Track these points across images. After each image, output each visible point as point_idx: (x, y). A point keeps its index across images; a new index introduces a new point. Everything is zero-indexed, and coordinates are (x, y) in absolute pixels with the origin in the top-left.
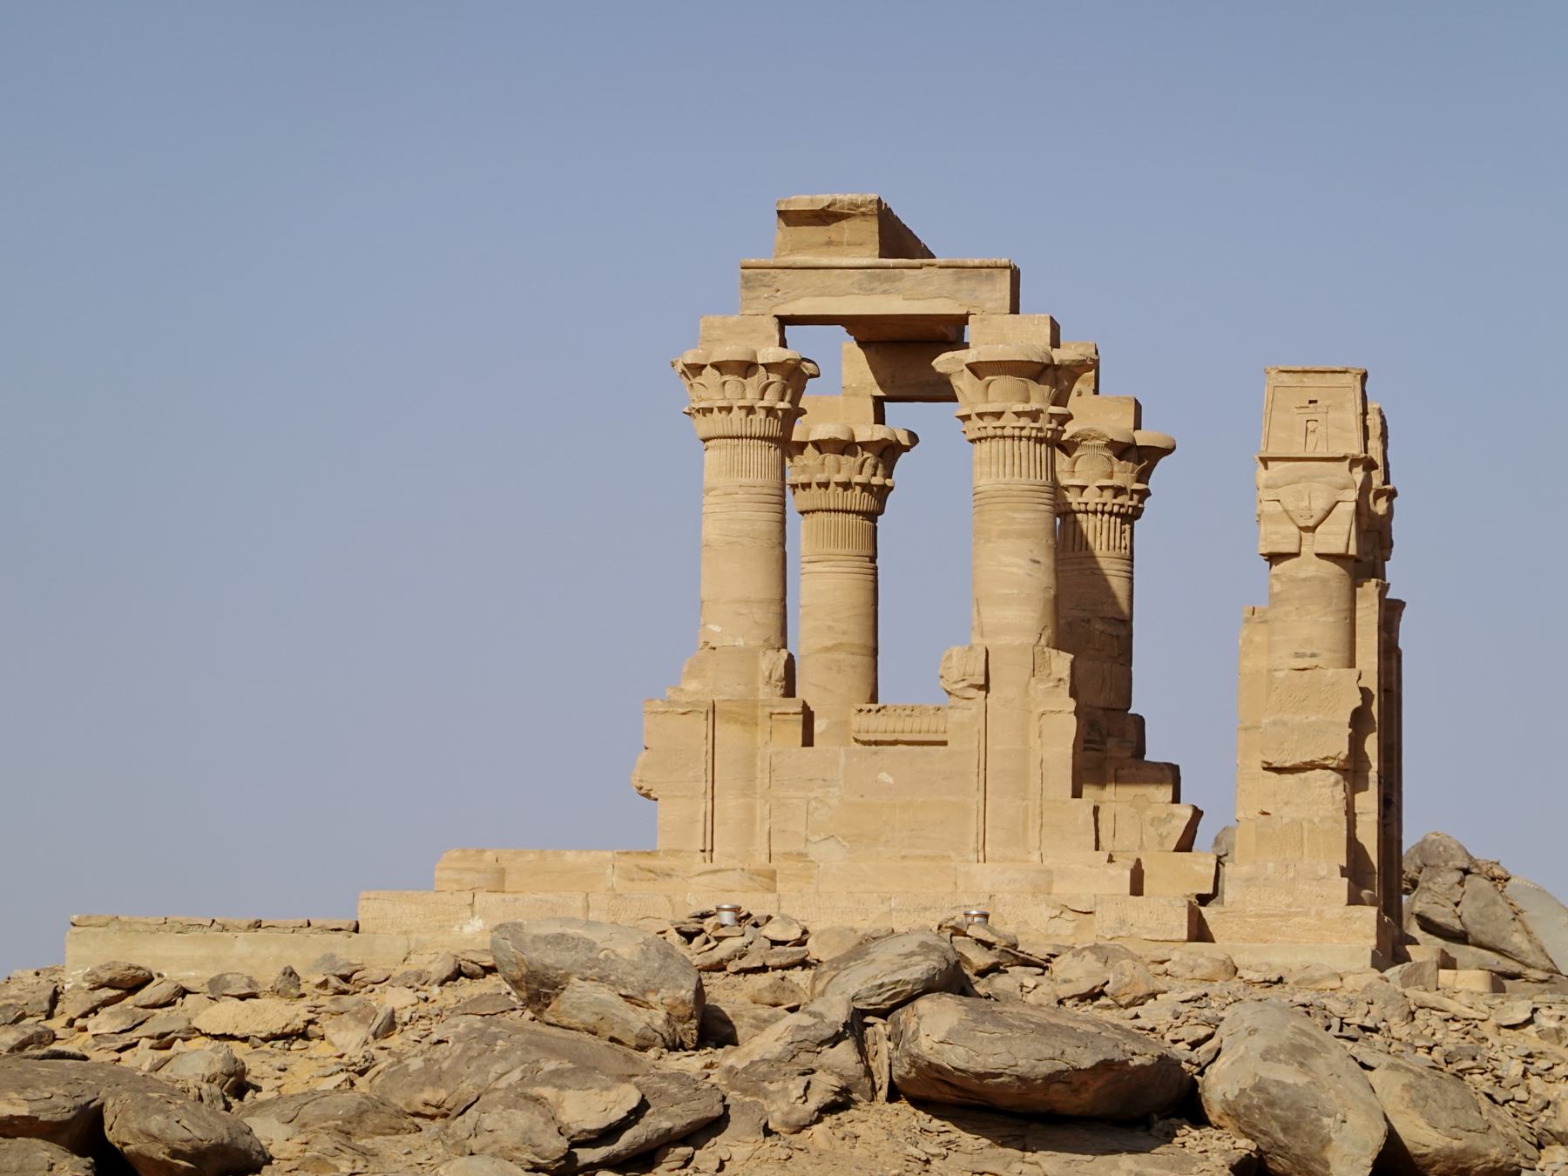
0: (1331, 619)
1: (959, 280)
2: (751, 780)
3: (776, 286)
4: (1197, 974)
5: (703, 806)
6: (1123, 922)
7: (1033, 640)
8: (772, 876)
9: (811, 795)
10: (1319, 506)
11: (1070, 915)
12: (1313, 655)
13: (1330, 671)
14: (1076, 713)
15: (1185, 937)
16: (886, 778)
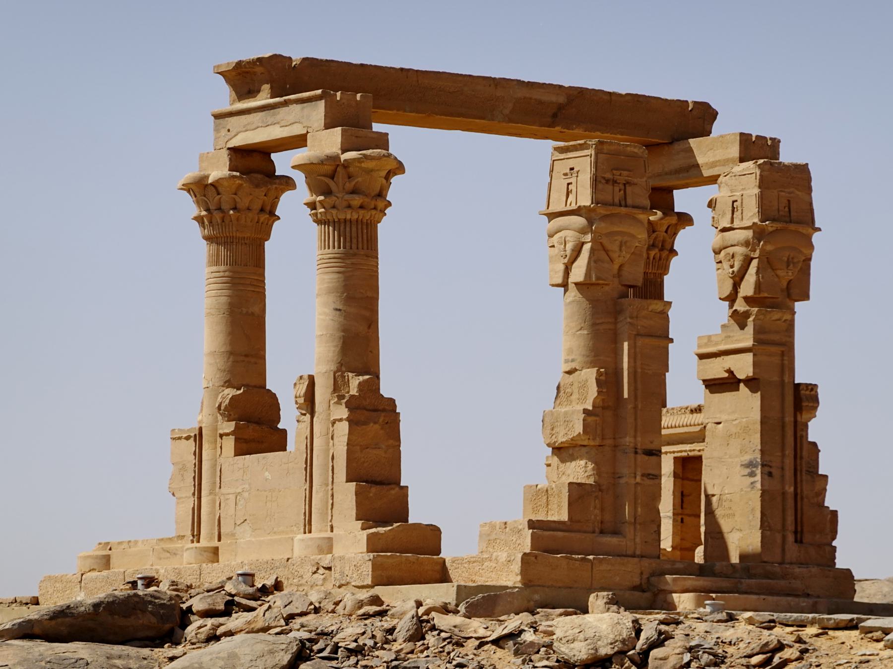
0: (586, 332)
1: (303, 109)
2: (215, 483)
3: (228, 127)
4: (346, 612)
5: (191, 502)
6: (342, 573)
7: (333, 367)
8: (215, 551)
9: (239, 490)
10: (569, 246)
11: (321, 571)
12: (573, 361)
13: (584, 371)
14: (349, 419)
15: (369, 581)
16: (267, 474)
